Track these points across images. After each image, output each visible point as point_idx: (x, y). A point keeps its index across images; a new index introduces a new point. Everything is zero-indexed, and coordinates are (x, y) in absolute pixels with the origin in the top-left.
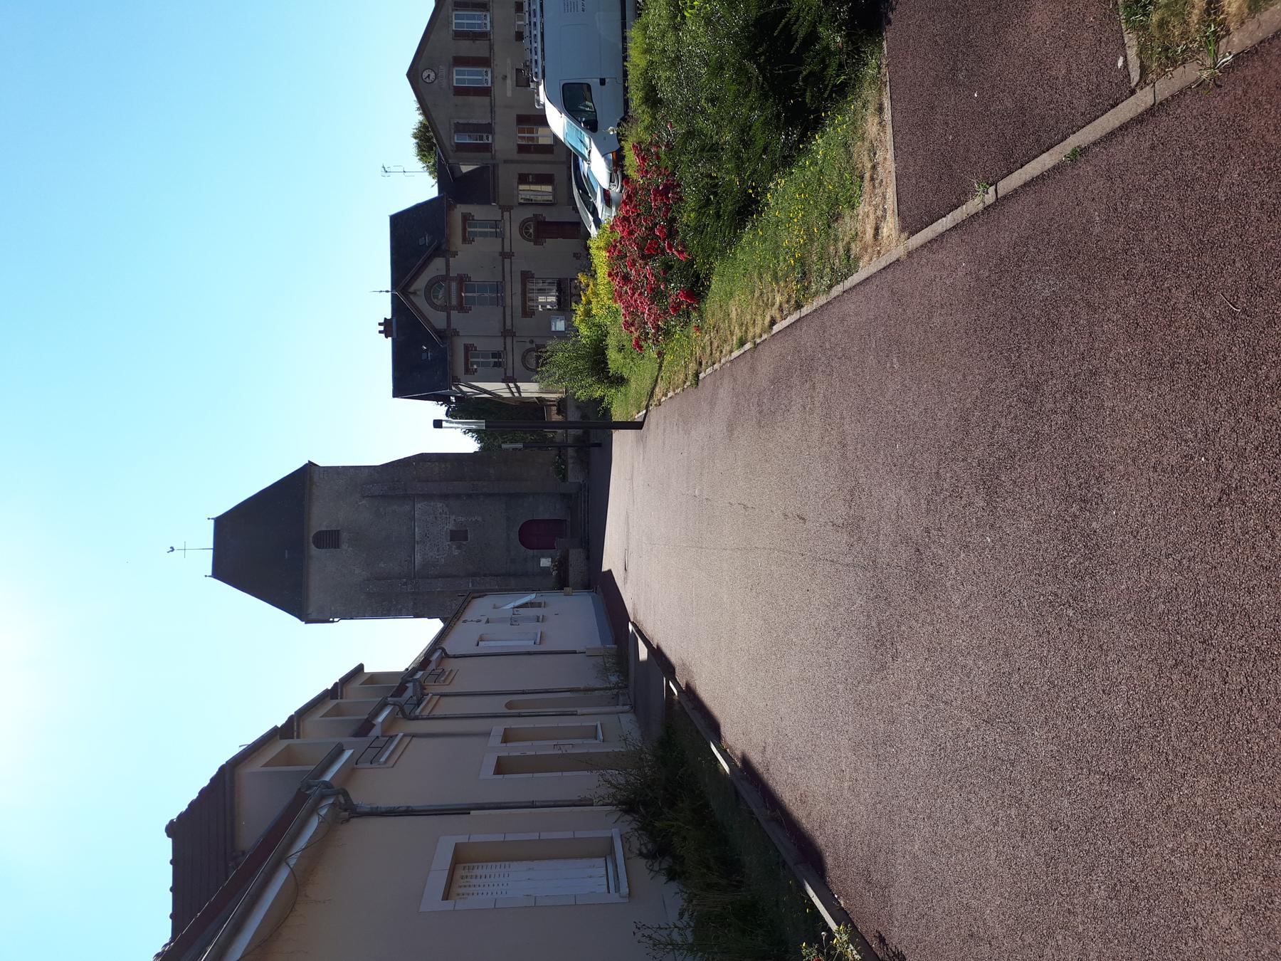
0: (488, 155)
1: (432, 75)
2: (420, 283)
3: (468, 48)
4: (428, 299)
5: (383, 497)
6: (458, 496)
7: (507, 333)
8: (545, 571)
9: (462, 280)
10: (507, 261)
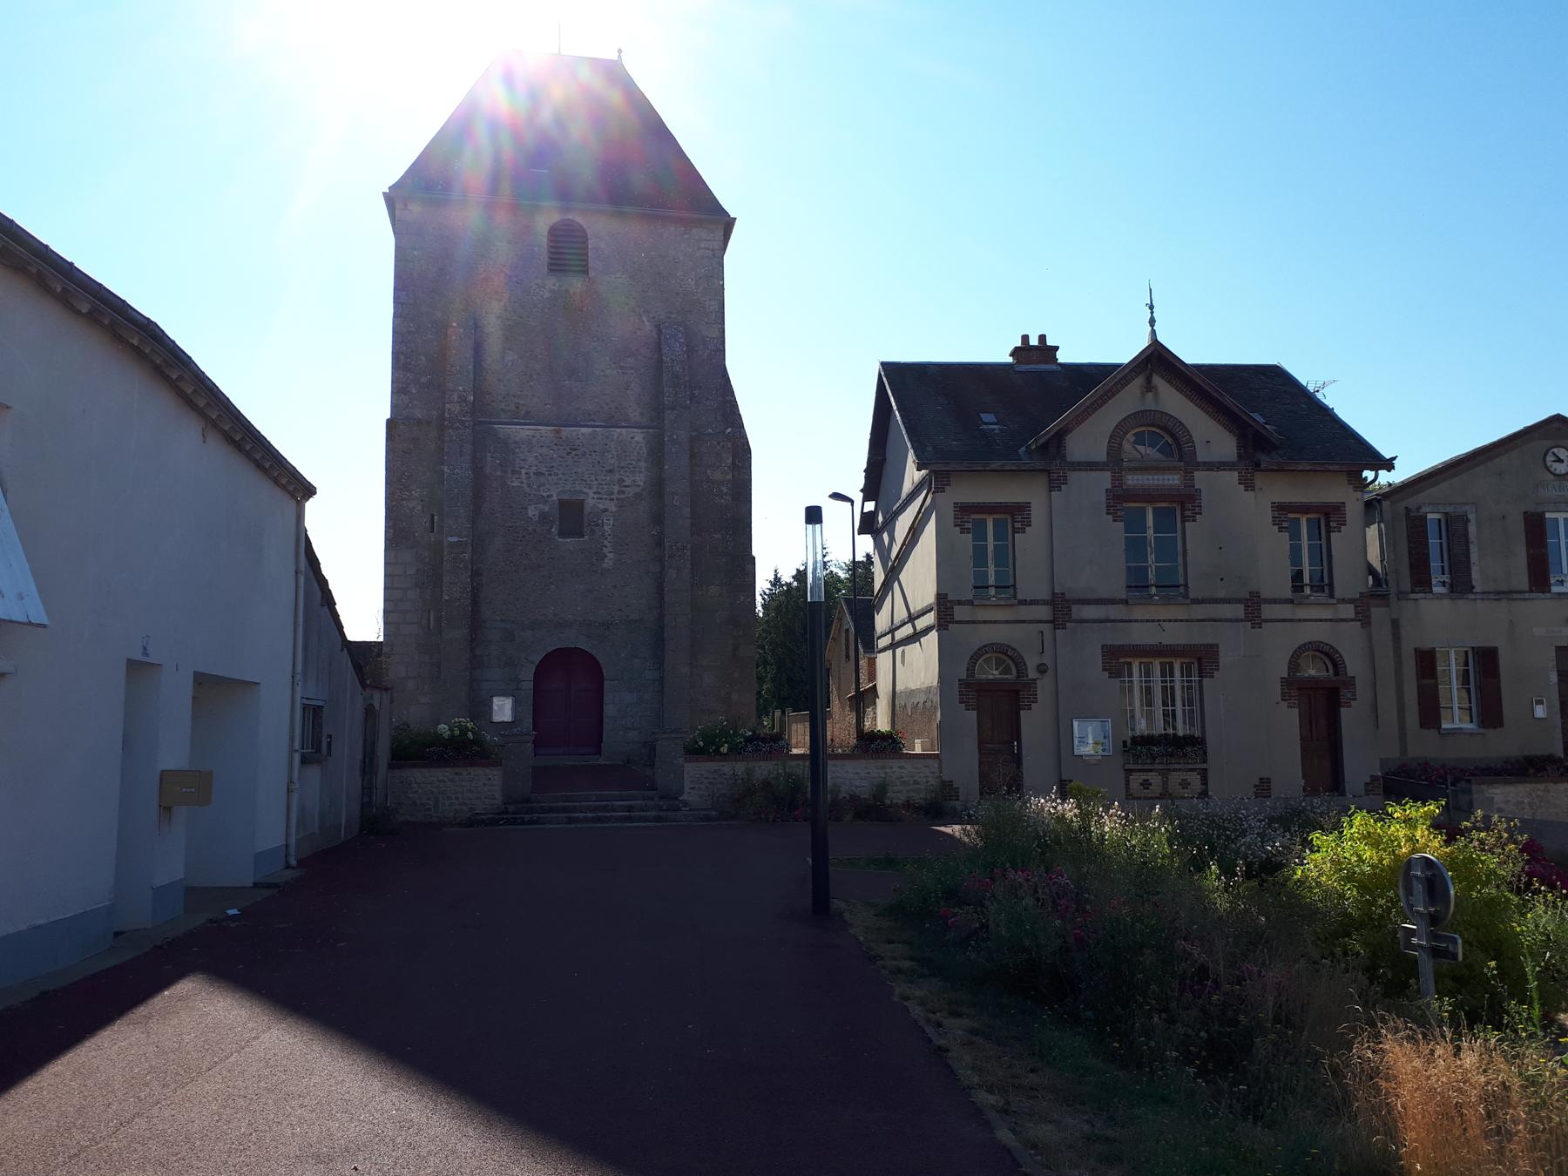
0: (1406, 584)
2: (1172, 401)
4: (1139, 418)
5: (660, 361)
6: (658, 519)
7: (1061, 608)
8: (480, 709)
9: (1185, 502)
10: (1239, 611)
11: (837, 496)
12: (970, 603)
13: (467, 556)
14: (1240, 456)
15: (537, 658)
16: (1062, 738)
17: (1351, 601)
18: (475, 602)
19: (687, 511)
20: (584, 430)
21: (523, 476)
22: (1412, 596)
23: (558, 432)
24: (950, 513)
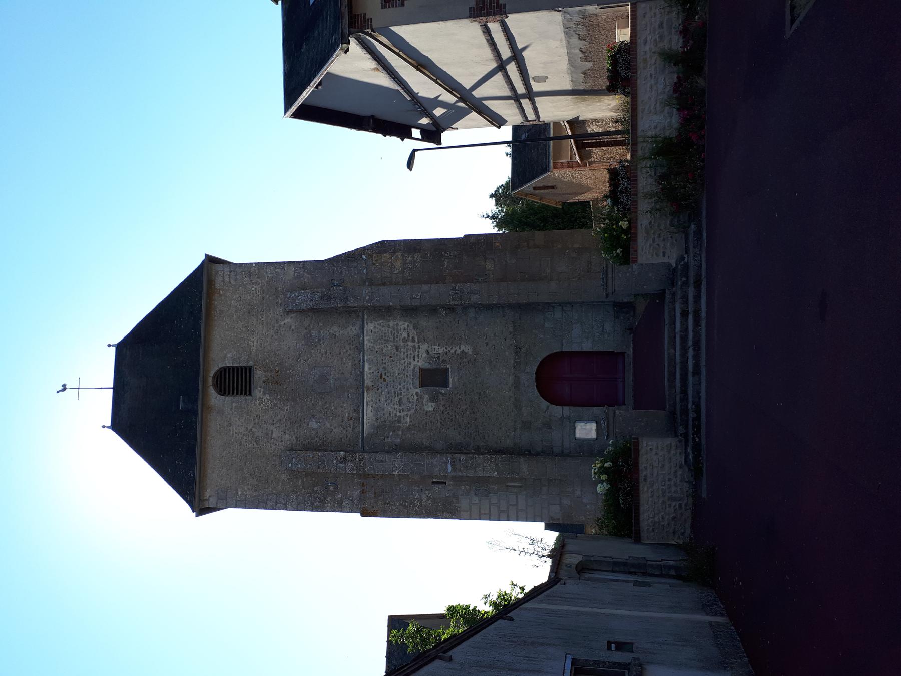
5: (315, 311)
6: (433, 310)
8: (586, 450)
11: (410, 165)
13: (463, 457)
15: (544, 403)
18: (500, 451)
19: (425, 287)
20: (366, 369)
21: (402, 414)
23: (368, 388)
24: (391, 11)
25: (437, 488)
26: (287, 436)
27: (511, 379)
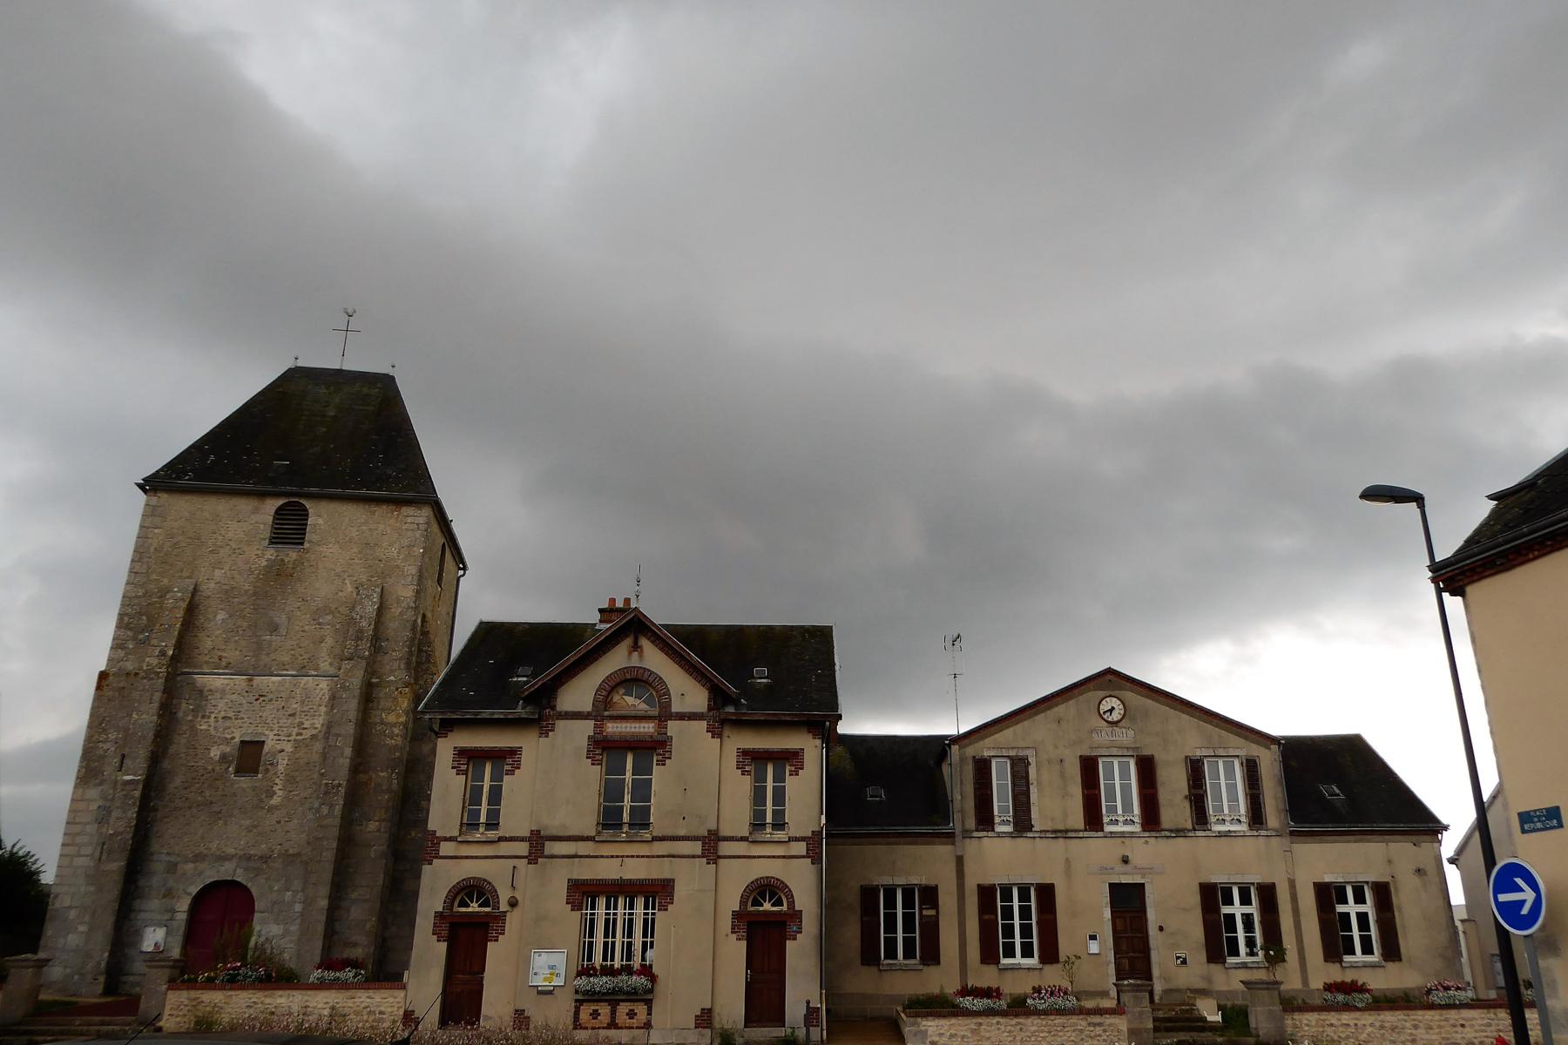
0: (971, 823)
1: (1116, 716)
2: (654, 659)
3: (1173, 783)
9: (652, 749)
10: (697, 848)
12: (743, 839)
14: (710, 709)
15: (194, 890)
16: (524, 964)
17: (802, 839)
19: (348, 752)
22: (976, 834)
25: (117, 760)
26: (212, 585)
27: (232, 851)
